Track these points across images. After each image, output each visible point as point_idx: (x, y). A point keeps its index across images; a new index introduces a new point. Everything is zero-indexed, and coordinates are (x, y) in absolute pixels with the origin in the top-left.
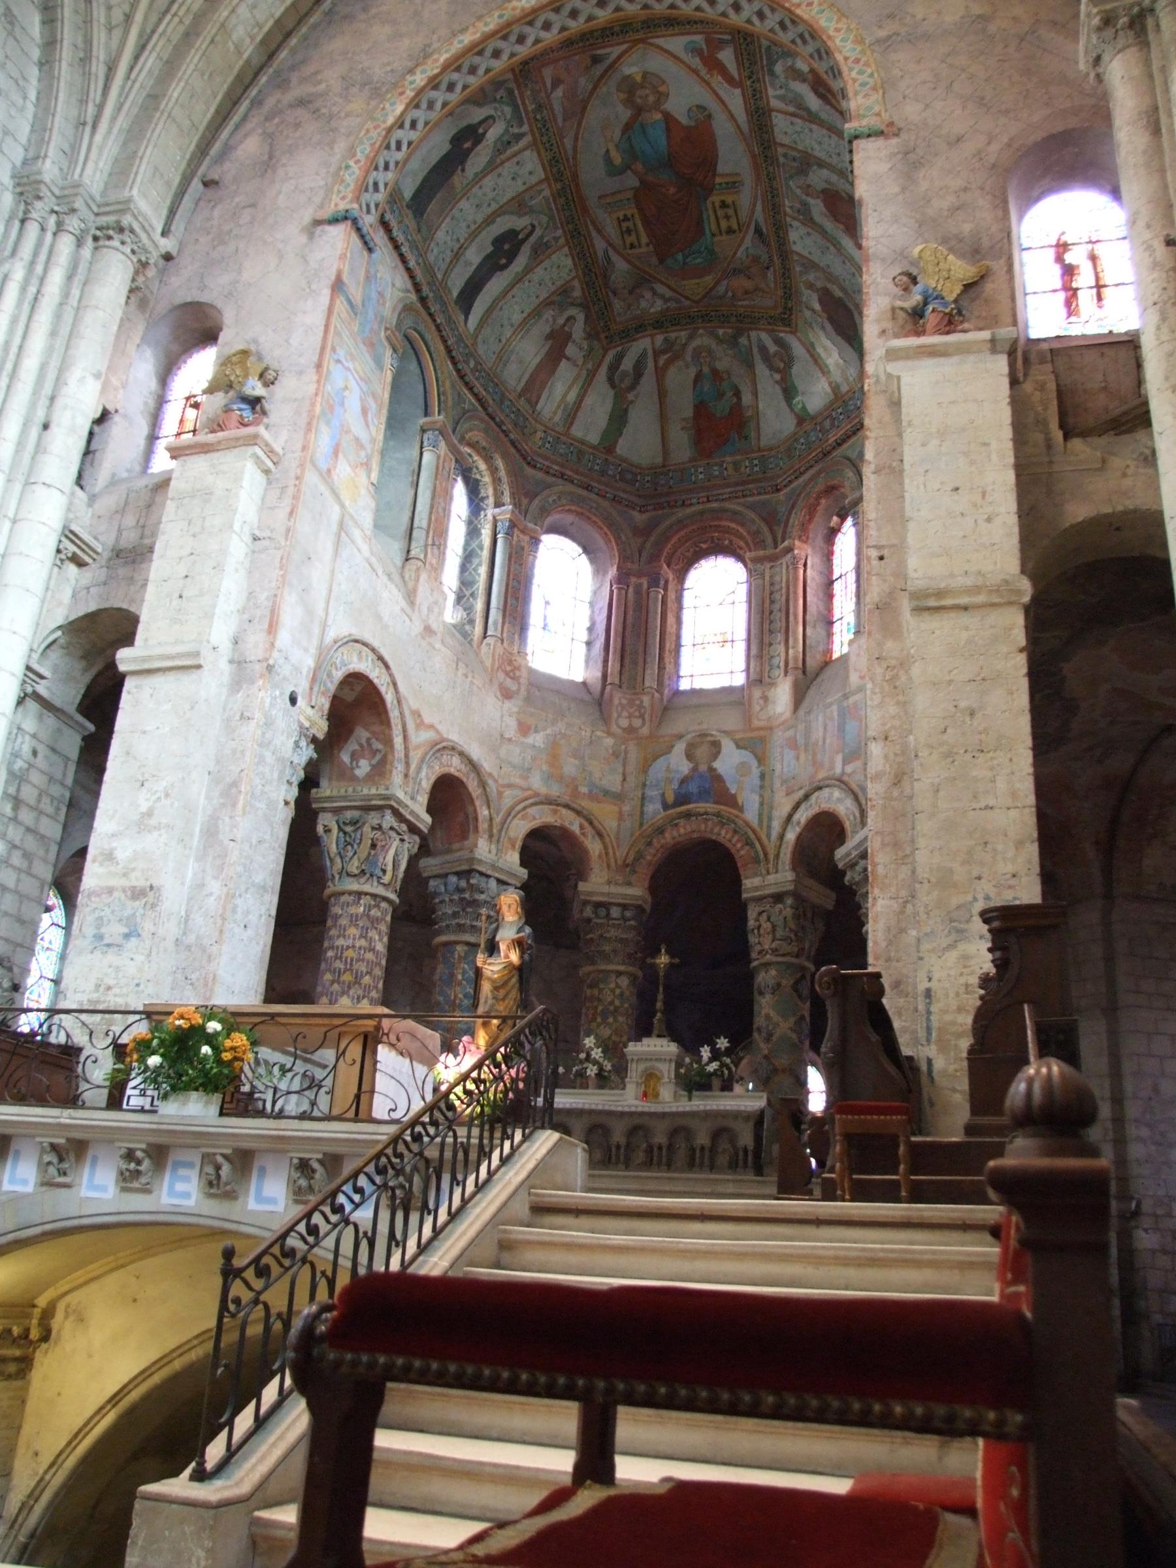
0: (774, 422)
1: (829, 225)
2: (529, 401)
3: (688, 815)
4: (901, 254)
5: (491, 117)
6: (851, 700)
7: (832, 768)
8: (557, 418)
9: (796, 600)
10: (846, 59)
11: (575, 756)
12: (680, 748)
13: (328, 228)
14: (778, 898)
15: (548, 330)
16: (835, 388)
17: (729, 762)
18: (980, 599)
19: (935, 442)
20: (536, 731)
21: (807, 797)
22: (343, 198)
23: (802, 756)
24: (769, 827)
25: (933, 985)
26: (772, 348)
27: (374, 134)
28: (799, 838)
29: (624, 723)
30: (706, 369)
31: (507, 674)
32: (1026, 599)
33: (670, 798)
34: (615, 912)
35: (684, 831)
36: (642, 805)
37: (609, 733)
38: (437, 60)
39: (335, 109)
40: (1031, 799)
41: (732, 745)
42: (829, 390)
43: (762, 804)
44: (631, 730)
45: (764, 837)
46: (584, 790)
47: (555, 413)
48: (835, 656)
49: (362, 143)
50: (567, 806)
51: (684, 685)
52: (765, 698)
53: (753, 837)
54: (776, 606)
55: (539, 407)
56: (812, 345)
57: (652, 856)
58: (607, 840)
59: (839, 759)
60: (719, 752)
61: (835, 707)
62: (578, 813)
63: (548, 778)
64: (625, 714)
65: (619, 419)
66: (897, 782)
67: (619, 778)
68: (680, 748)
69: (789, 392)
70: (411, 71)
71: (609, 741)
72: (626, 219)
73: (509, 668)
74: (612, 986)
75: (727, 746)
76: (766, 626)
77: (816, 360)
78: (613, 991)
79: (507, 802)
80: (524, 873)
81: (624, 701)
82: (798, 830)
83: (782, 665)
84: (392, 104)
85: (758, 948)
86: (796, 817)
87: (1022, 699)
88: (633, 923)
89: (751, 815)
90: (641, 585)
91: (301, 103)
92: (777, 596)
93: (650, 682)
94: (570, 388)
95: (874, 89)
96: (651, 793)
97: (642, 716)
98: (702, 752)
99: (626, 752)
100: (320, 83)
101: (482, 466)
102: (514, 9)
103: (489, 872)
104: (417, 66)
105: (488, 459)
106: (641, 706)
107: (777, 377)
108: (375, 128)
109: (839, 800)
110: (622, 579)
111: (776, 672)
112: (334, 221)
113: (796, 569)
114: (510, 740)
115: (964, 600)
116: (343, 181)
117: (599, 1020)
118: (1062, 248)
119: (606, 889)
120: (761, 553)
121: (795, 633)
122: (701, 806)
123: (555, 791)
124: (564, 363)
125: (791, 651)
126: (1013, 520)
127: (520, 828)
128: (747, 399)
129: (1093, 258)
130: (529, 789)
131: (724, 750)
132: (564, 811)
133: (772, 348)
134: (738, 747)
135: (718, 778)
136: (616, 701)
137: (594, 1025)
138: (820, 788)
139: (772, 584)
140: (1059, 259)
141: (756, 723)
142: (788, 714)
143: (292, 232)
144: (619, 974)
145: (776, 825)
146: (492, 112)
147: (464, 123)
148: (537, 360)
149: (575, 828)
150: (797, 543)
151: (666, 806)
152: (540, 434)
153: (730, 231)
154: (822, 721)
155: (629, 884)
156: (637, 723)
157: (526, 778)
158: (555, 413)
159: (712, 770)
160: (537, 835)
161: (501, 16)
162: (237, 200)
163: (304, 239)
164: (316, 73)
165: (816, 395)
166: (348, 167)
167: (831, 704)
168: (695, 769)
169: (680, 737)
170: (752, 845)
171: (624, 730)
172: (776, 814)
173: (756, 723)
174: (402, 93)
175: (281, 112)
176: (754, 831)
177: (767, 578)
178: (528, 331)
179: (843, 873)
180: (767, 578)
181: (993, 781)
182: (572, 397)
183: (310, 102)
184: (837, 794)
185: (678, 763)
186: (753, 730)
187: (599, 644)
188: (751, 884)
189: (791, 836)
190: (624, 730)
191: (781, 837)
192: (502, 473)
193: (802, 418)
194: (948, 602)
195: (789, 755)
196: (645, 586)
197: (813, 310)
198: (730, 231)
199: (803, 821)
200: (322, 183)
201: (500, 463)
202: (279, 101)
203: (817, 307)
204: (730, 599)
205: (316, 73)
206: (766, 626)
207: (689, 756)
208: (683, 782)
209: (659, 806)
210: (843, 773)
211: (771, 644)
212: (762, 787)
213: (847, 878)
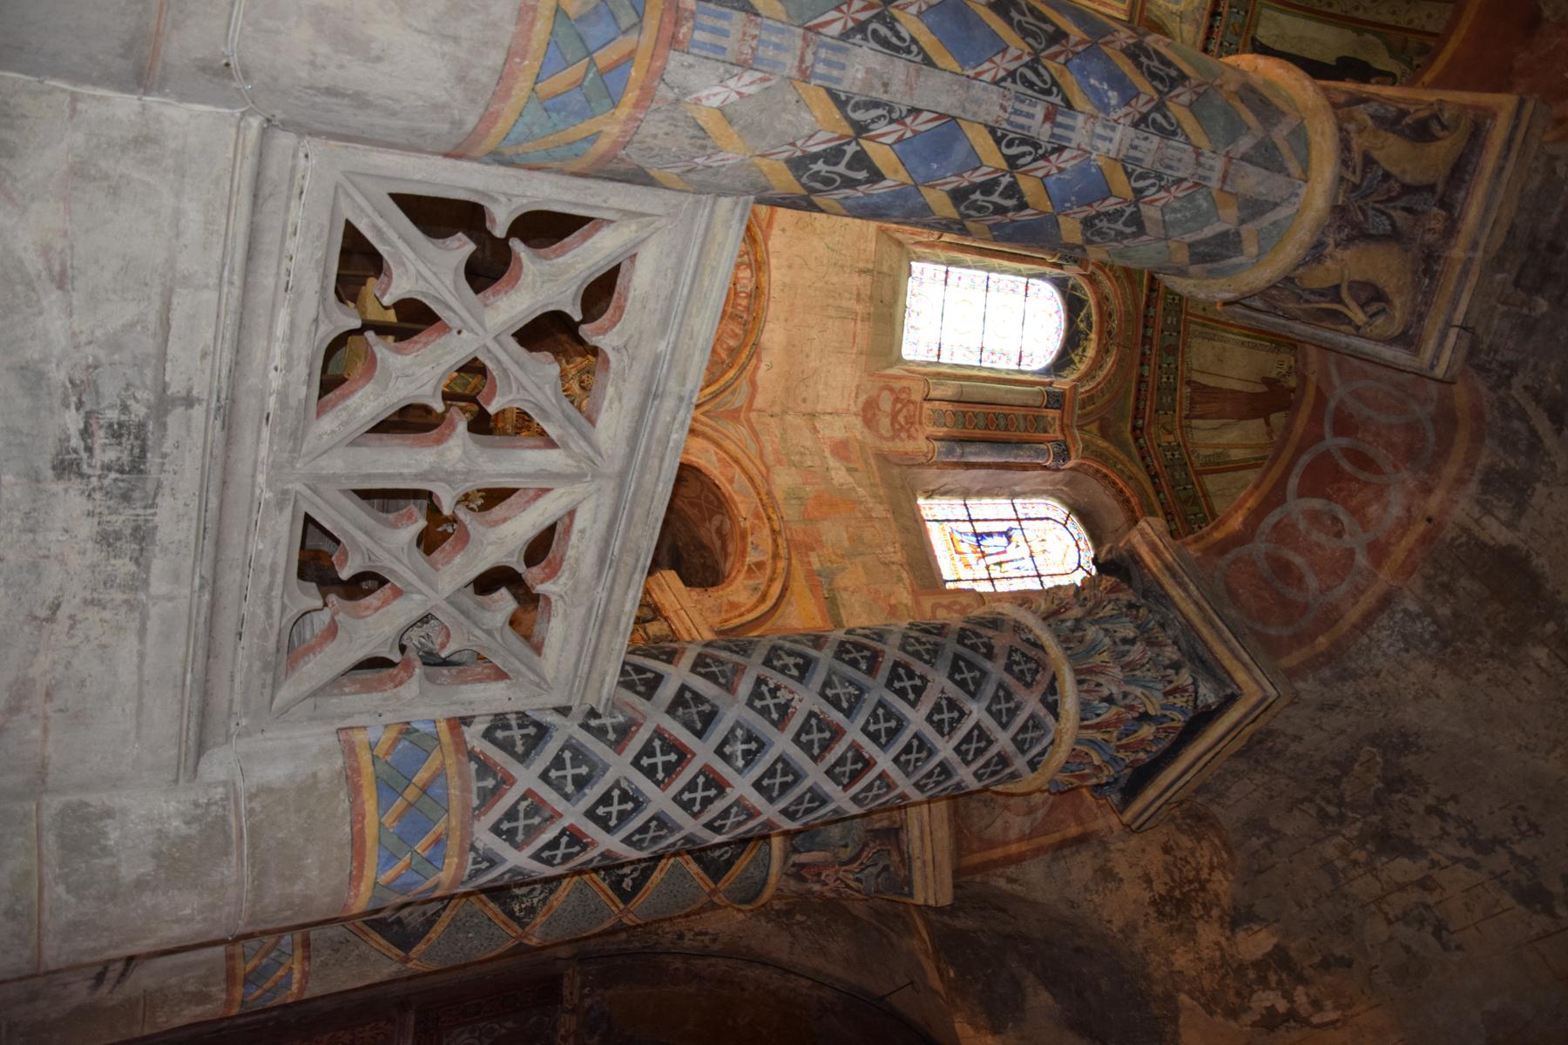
2: (1193, 403)
5: (1393, 75)
8: (1203, 452)
11: (851, 539)
15: (1273, 375)
20: (849, 470)
47: (1207, 446)
55: (1195, 422)
63: (794, 495)
73: (901, 419)
94: (1245, 447)
101: (1091, 352)
105: (1103, 350)
124: (1262, 421)
146: (1398, 74)
147: (1363, 57)
148: (1237, 386)
152: (1171, 438)
157: (780, 462)
158: (1207, 446)
178: (1254, 347)
182: (1237, 454)
192: (1102, 374)
201: (1110, 361)
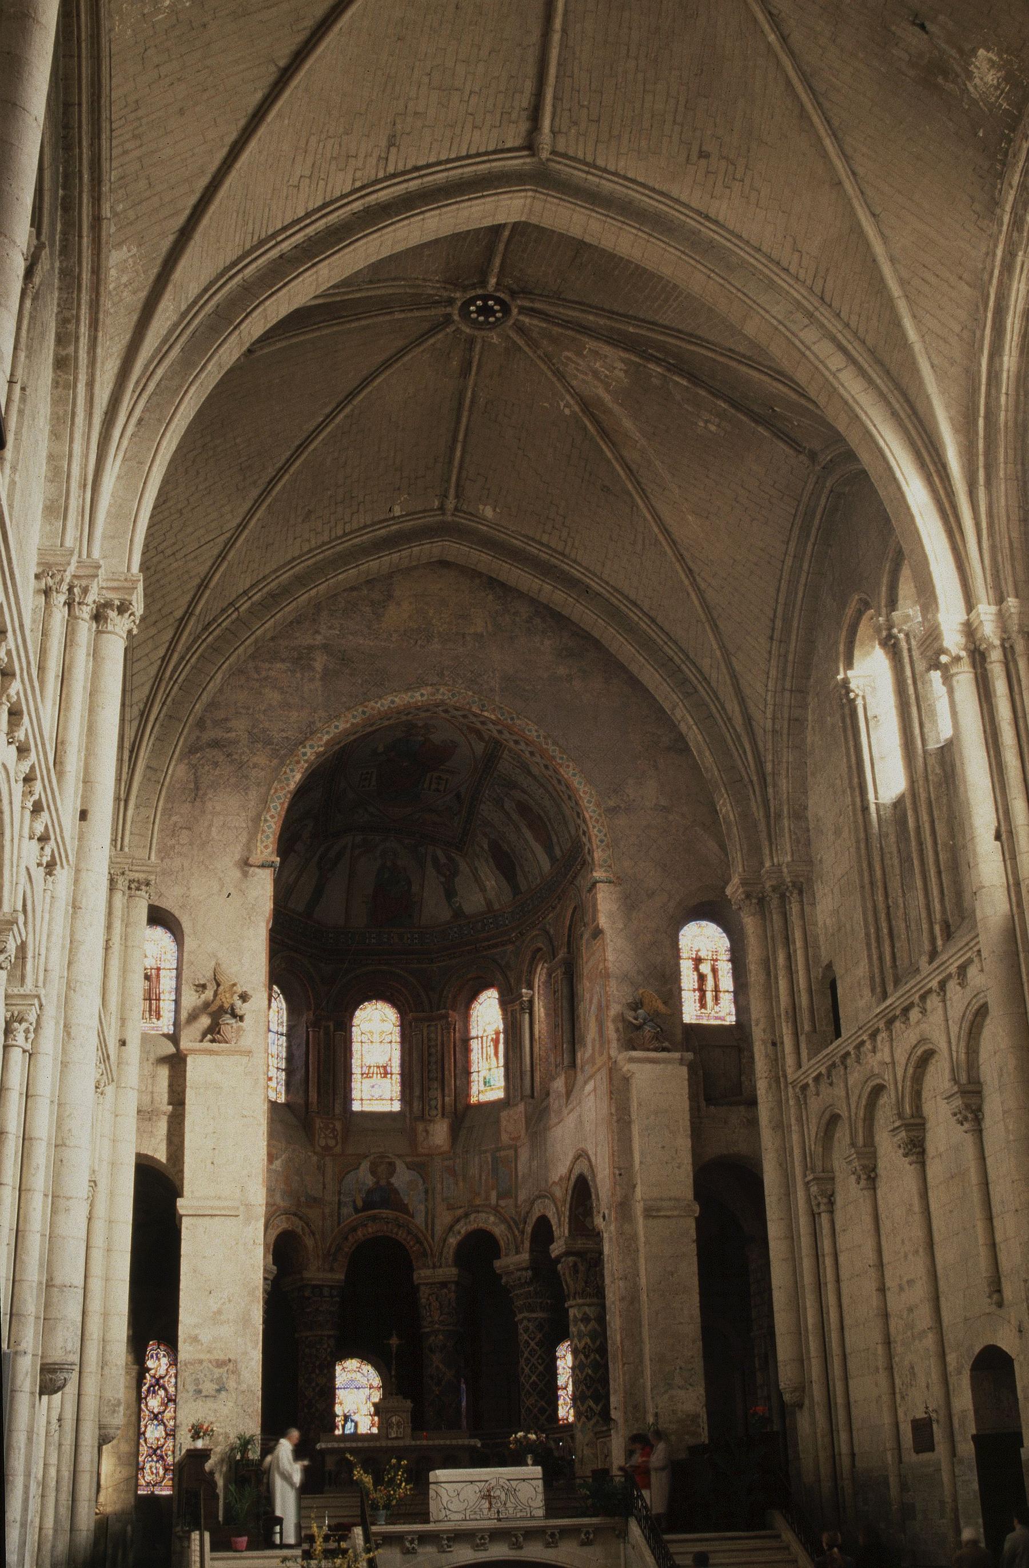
0: (434, 909)
1: (515, 816)
3: (374, 1218)
4: (626, 976)
6: (503, 1153)
7: (487, 1198)
9: (450, 1058)
10: (591, 817)
12: (365, 1165)
13: (257, 870)
14: (444, 1285)
16: (489, 903)
17: (402, 1178)
18: (676, 1213)
19: (653, 1117)
20: (277, 1159)
21: (467, 1215)
22: (266, 847)
23: (461, 1184)
24: (433, 1229)
25: (659, 1410)
26: (443, 860)
27: (281, 794)
28: (460, 1244)
29: (323, 1143)
30: (389, 864)
32: (697, 1215)
33: (360, 1204)
34: (326, 1292)
36: (339, 1208)
38: (321, 739)
39: (245, 758)
40: (699, 1320)
41: (404, 1166)
42: (483, 903)
43: (427, 1213)
44: (327, 1148)
45: (430, 1239)
46: (303, 1199)
48: (473, 1100)
49: (273, 801)
50: (295, 1214)
51: (356, 1107)
52: (427, 1132)
53: (422, 1238)
54: (433, 1059)
56: (476, 869)
59: (494, 1194)
60: (394, 1171)
61: (488, 1155)
62: (301, 1218)
64: (323, 1135)
65: (318, 892)
66: (632, 1303)
67: (321, 1186)
68: (365, 1165)
69: (450, 893)
70: (302, 743)
71: (315, 1158)
72: (367, 773)
74: (325, 1346)
76: (425, 1074)
77: (477, 879)
78: (325, 1350)
82: (459, 1238)
83: (439, 1106)
84: (292, 770)
85: (430, 1319)
86: (457, 1227)
87: (695, 1268)
88: (337, 1299)
89: (420, 1220)
90: (329, 1027)
91: (216, 744)
92: (433, 1050)
93: (338, 1109)
95: (608, 846)
96: (343, 1199)
97: (335, 1137)
99: (325, 1164)
100: (229, 730)
102: (373, 708)
104: (306, 739)
106: (334, 1129)
107: (443, 879)
108: (282, 788)
109: (494, 1224)
110: (315, 1024)
111: (434, 1113)
112: (263, 866)
113: (449, 1033)
115: (668, 1214)
116: (264, 831)
117: (317, 1371)
118: (698, 961)
119: (321, 1275)
120: (421, 1015)
121: (450, 1085)
122: (385, 1213)
124: (292, 854)
125: (447, 1099)
126: (690, 1168)
128: (415, 888)
129: (714, 971)
131: (398, 1169)
132: (293, 1218)
133: (443, 860)
134: (408, 1168)
135: (396, 1192)
136: (317, 1126)
137: (314, 1376)
138: (478, 1212)
139: (429, 1040)
140: (696, 969)
141: (420, 1150)
142: (446, 1148)
143: (227, 864)
144: (329, 1337)
149: (299, 1230)
150: (450, 1012)
151: (357, 1210)
153: (438, 790)
155: (332, 1270)
156: (331, 1143)
159: (389, 1184)
161: (364, 713)
162: (174, 818)
163: (237, 874)
164: (227, 719)
165: (472, 902)
166: (266, 821)
167: (486, 1152)
168: (377, 1183)
170: (421, 1244)
171: (323, 1148)
172: (437, 1221)
173: (420, 1150)
174: (298, 762)
175: (200, 749)
176: (422, 1232)
177: (425, 1034)
179: (500, 1277)
180: (425, 1034)
181: (682, 1310)
183: (225, 746)
184: (492, 1219)
185: (364, 1176)
186: (418, 1155)
187: (299, 1075)
188: (422, 1274)
189: (453, 1241)
190: (323, 1148)
191: (445, 1240)
193: (458, 913)
194: (662, 1214)
196: (332, 1028)
197: (482, 847)
198: (438, 790)
199: (463, 1231)
200: (244, 825)
202: (198, 738)
203: (486, 847)
204: (388, 1039)
205: (227, 719)
206: (425, 1074)
207: (373, 1173)
208: (370, 1192)
209: (351, 1209)
210: (497, 1205)
211: (429, 1089)
212: (426, 1200)
213: (503, 1281)
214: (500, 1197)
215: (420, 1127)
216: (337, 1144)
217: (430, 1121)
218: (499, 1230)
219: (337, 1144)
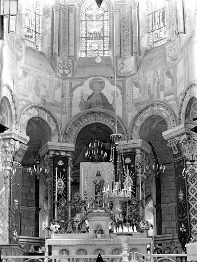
7: (159, 96)
12: (87, 83)
17: (109, 90)
31: (18, 49)
35: (91, 120)
37: (57, 76)
52: (123, 64)
57: (76, 131)
58: (58, 123)
64: (61, 67)
68: (87, 83)
71: (56, 79)
75: (107, 82)
79: (20, 107)
80: (28, 138)
81: (61, 62)
89: (119, 112)
98: (97, 86)
103: (17, 139)
114: (20, 79)
123: (38, 101)
127: (25, 118)
130: (28, 101)
145: (130, 119)
154: (149, 76)
156: (67, 72)
159: (101, 94)
160: (30, 122)
169: (86, 78)
185: (85, 90)
195: (136, 90)
207: (91, 87)
214: (166, 95)
215: (119, 62)
216: (70, 72)
217: (125, 58)
218: (165, 114)
219: (70, 72)
